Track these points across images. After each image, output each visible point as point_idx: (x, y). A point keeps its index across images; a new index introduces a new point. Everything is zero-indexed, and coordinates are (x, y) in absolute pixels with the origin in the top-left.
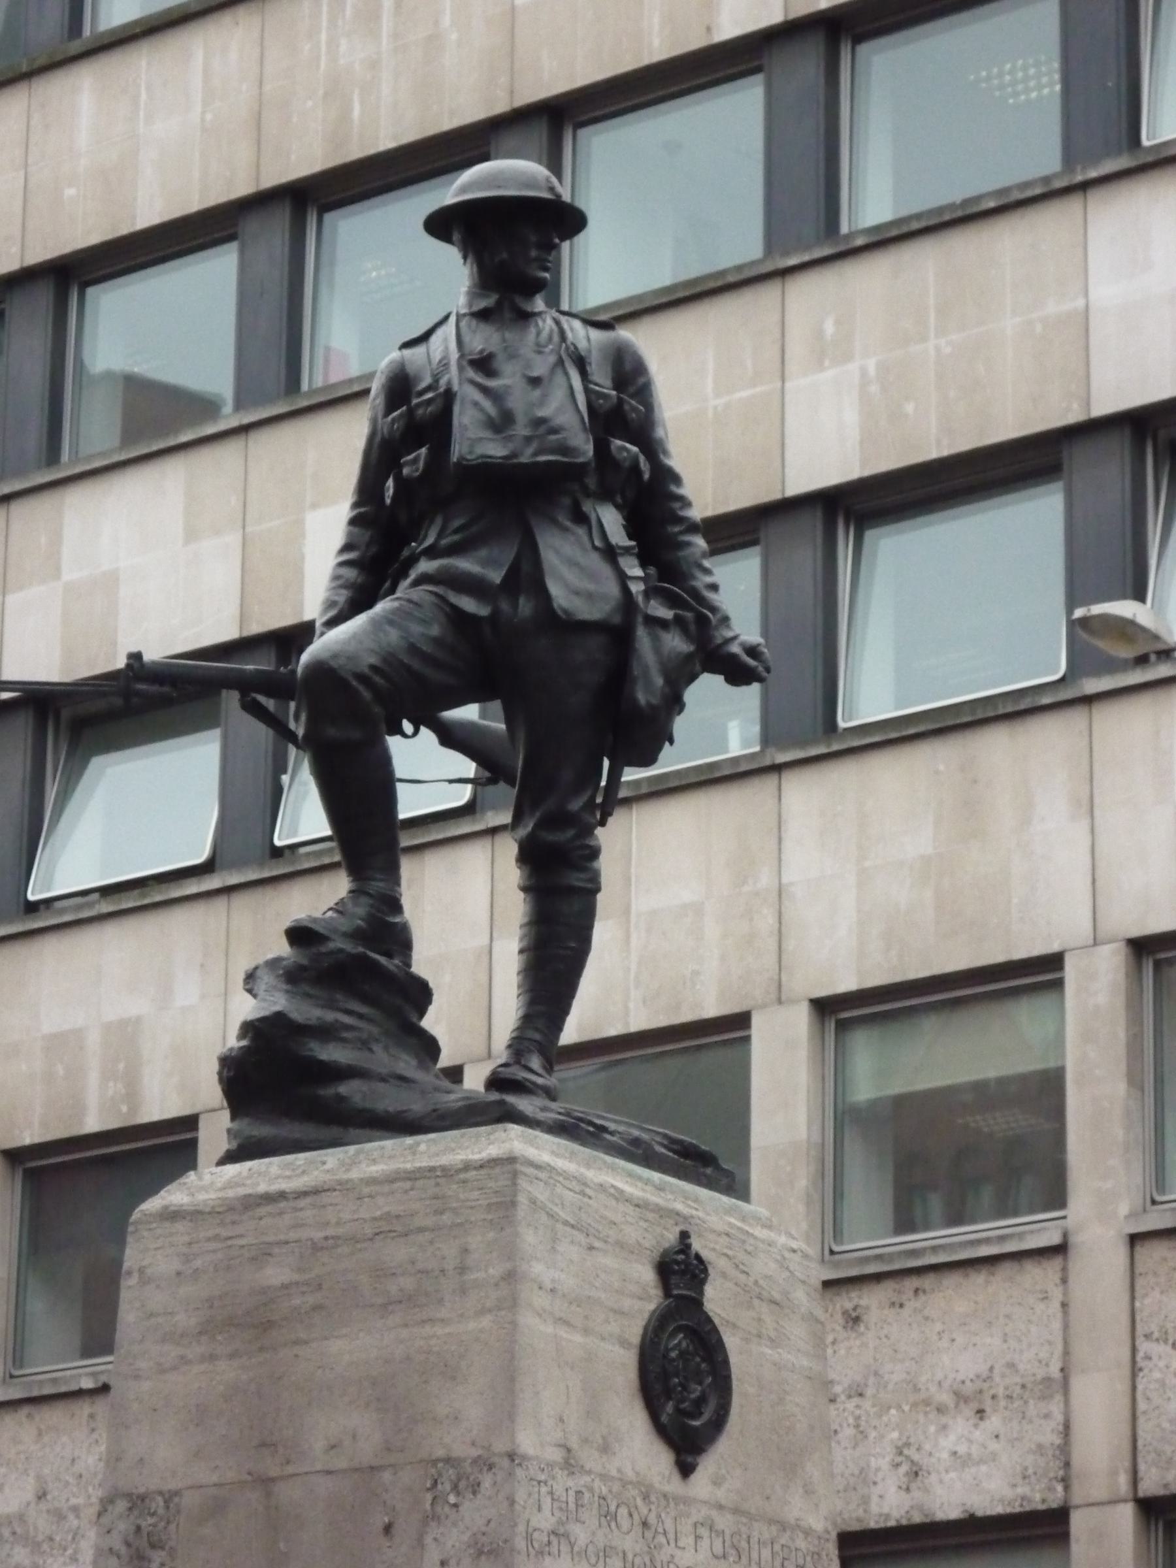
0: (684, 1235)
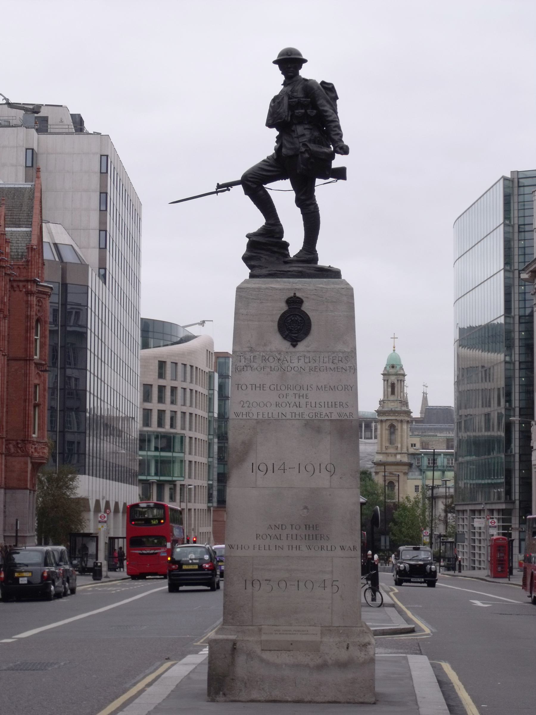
0: (295, 294)
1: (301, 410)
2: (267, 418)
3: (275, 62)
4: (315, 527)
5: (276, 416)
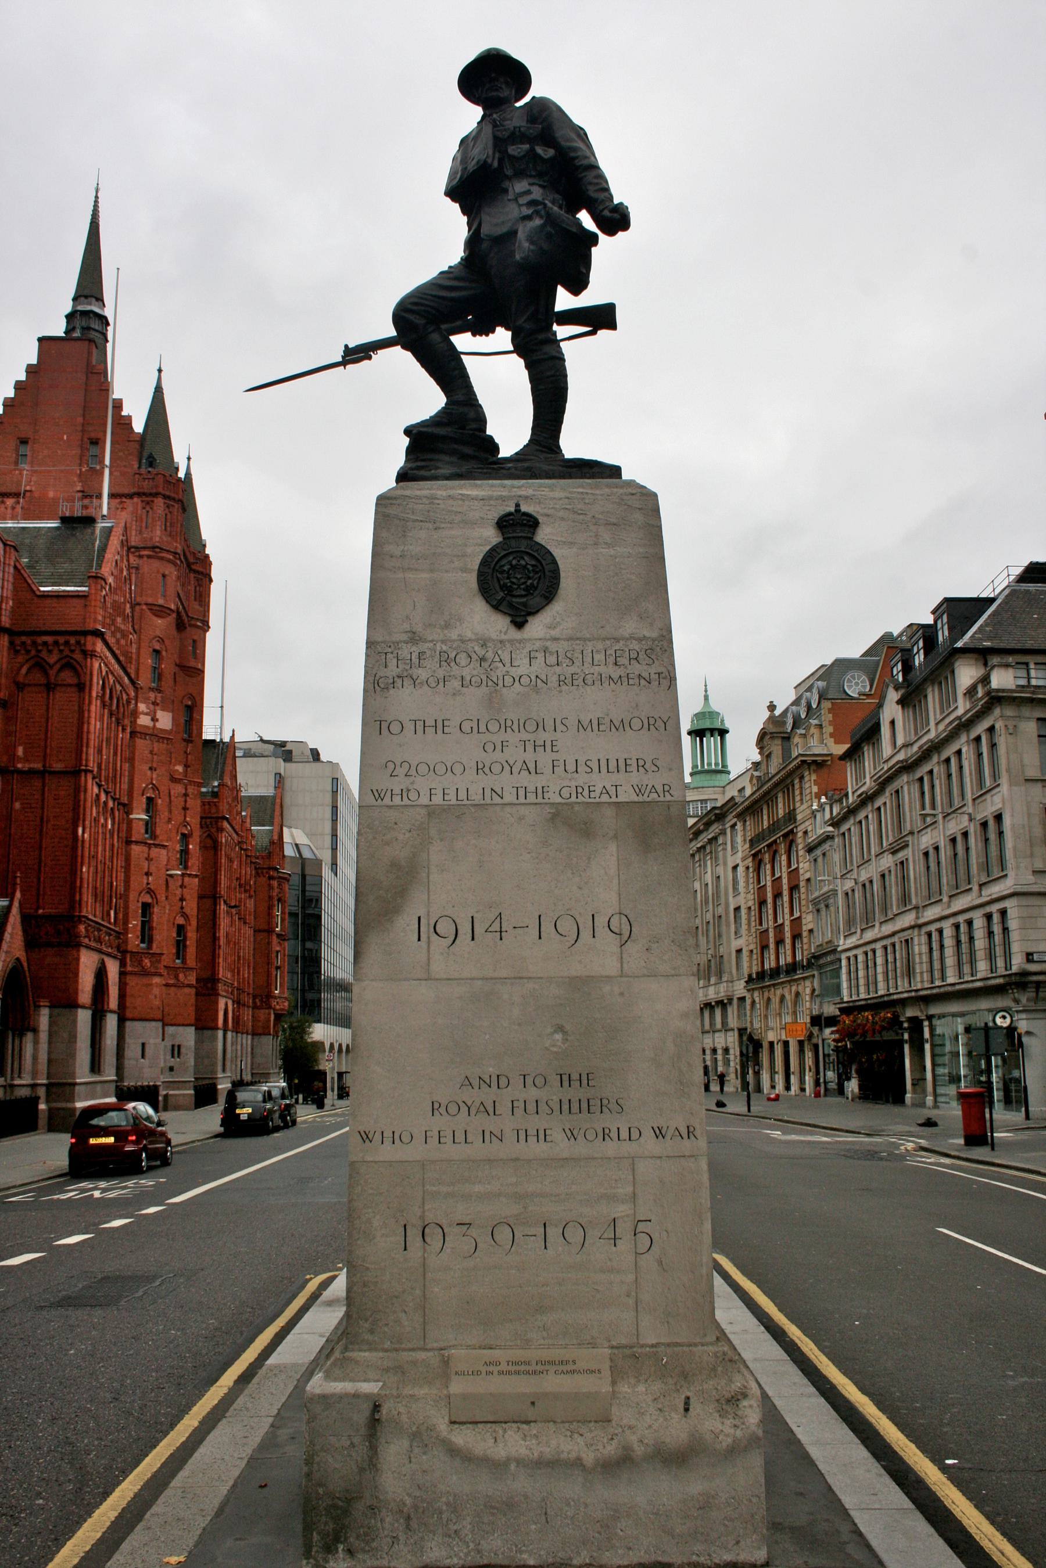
0: (517, 505)
1: (540, 781)
2: (454, 802)
4: (586, 1079)
5: (477, 798)
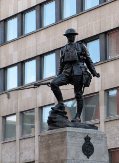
3: (64, 35)
